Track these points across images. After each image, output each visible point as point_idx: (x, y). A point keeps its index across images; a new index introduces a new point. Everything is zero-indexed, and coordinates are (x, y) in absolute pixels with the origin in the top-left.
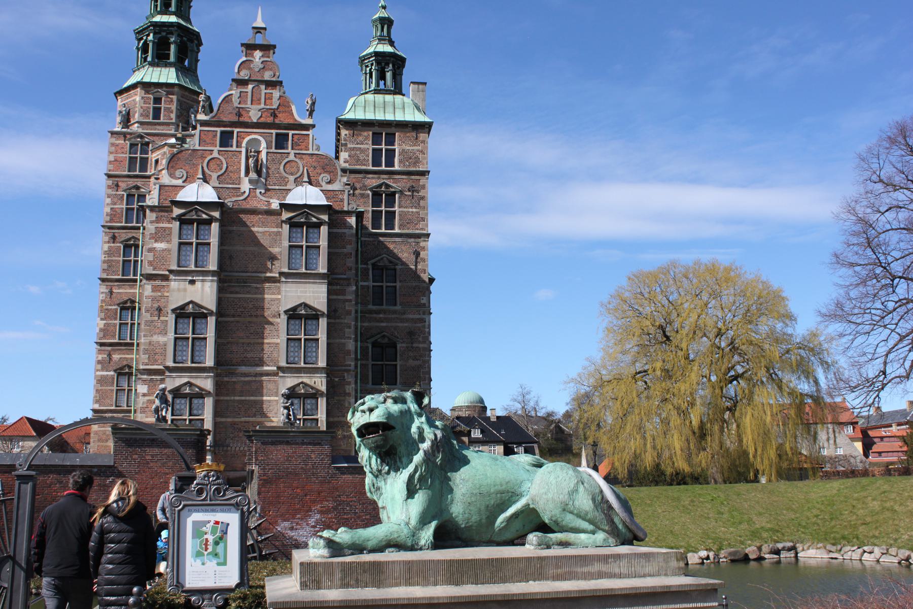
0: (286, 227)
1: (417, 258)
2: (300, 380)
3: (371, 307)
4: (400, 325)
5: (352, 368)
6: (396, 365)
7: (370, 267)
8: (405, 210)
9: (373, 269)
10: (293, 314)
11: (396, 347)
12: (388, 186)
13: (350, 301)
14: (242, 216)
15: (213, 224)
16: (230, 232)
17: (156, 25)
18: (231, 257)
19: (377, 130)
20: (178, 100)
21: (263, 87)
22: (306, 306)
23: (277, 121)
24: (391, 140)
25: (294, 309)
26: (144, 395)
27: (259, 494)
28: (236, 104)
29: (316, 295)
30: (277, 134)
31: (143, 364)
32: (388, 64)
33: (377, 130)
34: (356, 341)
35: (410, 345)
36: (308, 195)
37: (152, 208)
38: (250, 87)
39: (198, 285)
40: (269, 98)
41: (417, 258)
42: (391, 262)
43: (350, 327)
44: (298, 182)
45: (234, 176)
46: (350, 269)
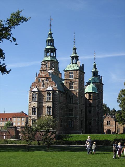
5: (57, 115)
10: (47, 107)
12: (72, 82)
14: (42, 92)
17: (46, 49)
20: (50, 63)
21: (44, 71)
24: (72, 73)
25: (48, 106)
26: (29, 120)
29: (50, 104)
36: (50, 89)
40: (45, 73)
44: (49, 86)
45: (40, 86)
46: (57, 99)
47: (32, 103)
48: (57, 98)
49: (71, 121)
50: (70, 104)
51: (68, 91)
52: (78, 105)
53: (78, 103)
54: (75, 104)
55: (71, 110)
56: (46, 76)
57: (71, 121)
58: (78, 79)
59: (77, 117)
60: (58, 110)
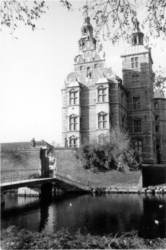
0: (97, 90)
1: (146, 94)
2: (102, 133)
3: (133, 110)
4: (142, 114)
6: (141, 127)
7: (132, 98)
8: (142, 80)
9: (133, 99)
10: (99, 115)
11: (141, 121)
13: (117, 109)
15: (78, 91)
16: (84, 93)
18: (84, 101)
19: (132, 57)
21: (90, 51)
22: (103, 112)
23: (95, 60)
27: (56, 166)
28: (84, 58)
29: (105, 108)
30: (95, 65)
31: (64, 131)
32: (137, 36)
33: (132, 57)
34: (119, 121)
35: (145, 120)
37: (64, 90)
38: (87, 52)
39: (75, 109)
40: (92, 55)
41: (146, 94)
42: (138, 96)
43: (117, 117)
45: (84, 78)
46: (117, 100)
47: (70, 109)
48: (117, 98)
49: (138, 141)
50: (136, 111)
51: (129, 89)
52: (150, 112)
53: (149, 110)
54: (144, 110)
55: (138, 121)
56: (94, 59)
57: (138, 141)
58: (147, 68)
59: (150, 134)
60: (119, 119)
